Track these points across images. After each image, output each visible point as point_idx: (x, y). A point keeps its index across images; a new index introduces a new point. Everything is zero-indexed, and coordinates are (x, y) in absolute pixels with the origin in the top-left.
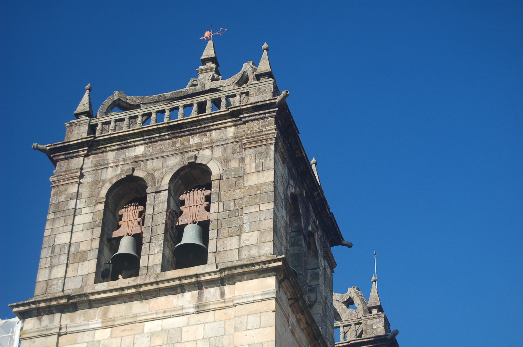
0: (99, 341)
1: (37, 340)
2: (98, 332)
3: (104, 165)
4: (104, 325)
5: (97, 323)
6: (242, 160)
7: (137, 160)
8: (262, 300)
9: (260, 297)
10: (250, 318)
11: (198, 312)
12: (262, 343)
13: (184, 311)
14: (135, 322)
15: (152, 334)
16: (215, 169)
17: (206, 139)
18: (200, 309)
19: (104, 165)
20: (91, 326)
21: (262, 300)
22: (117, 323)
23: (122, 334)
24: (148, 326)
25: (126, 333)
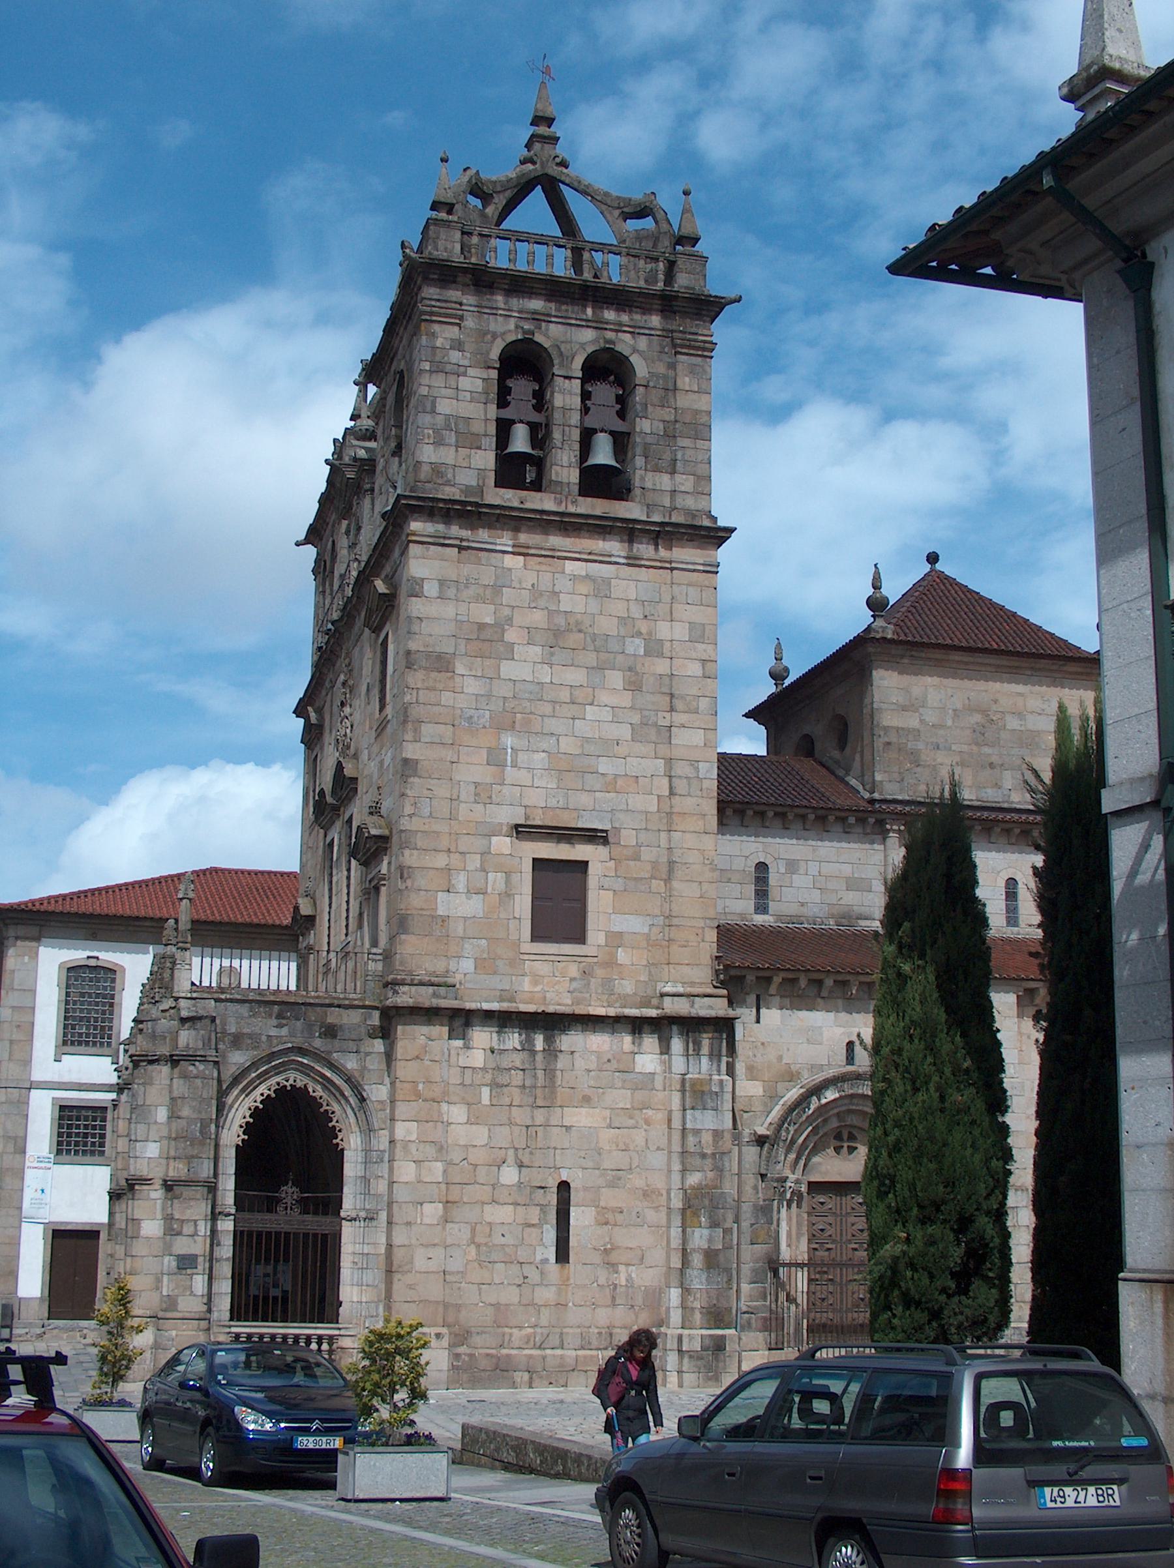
0: (510, 570)
1: (432, 547)
2: (508, 557)
3: (493, 308)
4: (517, 550)
5: (506, 545)
6: (672, 366)
7: (538, 318)
8: (704, 571)
9: (701, 568)
10: (691, 589)
11: (628, 565)
12: (704, 625)
13: (613, 559)
14: (553, 557)
15: (574, 578)
16: (641, 368)
17: (625, 318)
18: (633, 561)
19: (493, 308)
20: (498, 548)
21: (704, 571)
22: (532, 551)
23: (538, 567)
24: (570, 566)
25: (544, 568)
